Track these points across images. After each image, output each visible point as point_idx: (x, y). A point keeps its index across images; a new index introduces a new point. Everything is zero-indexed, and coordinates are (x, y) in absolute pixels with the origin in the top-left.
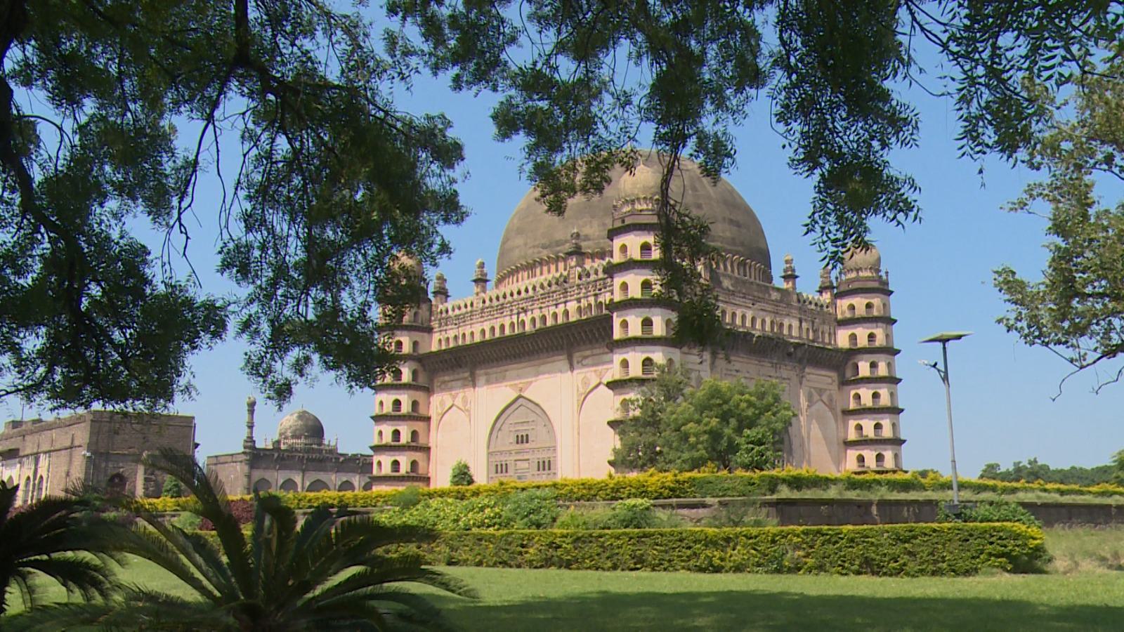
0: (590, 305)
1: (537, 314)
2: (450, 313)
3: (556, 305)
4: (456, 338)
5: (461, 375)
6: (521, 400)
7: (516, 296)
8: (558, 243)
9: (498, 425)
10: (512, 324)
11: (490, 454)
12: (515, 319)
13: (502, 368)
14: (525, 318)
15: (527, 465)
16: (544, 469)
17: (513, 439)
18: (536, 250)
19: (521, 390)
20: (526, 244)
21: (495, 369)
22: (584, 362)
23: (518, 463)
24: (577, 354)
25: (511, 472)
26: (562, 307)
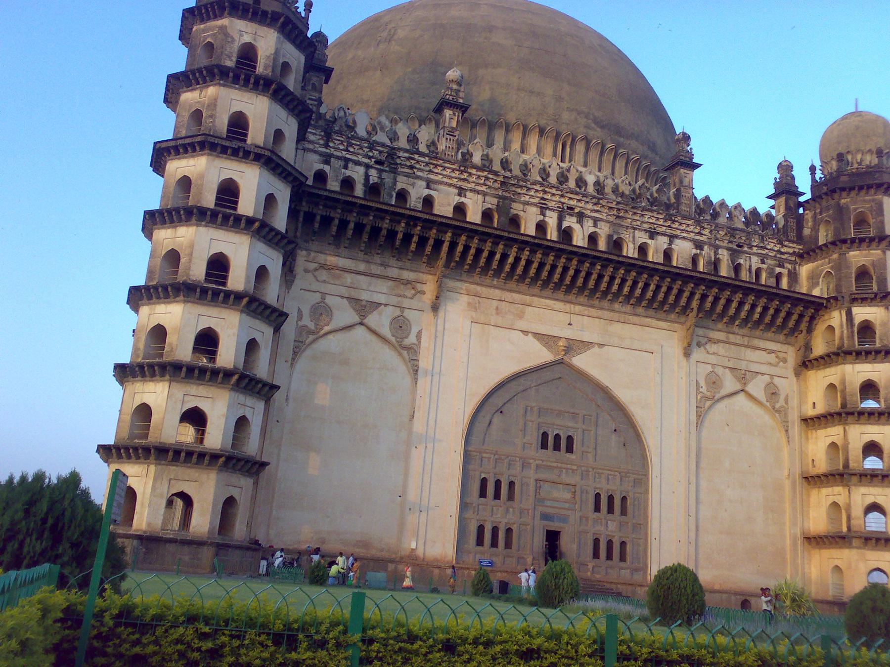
0: (716, 264)
1: (603, 230)
2: (361, 131)
3: (652, 235)
4: (373, 190)
5: (393, 272)
6: (558, 368)
7: (553, 179)
8: (618, 131)
9: (498, 401)
10: (541, 227)
11: (467, 457)
12: (552, 220)
13: (517, 297)
14: (576, 227)
15: (568, 496)
16: (611, 510)
17: (534, 438)
18: (583, 121)
19: (568, 350)
20: (559, 99)
21: (497, 292)
22: (708, 346)
23: (546, 487)
24: (700, 331)
25: (525, 499)
26: (662, 242)
